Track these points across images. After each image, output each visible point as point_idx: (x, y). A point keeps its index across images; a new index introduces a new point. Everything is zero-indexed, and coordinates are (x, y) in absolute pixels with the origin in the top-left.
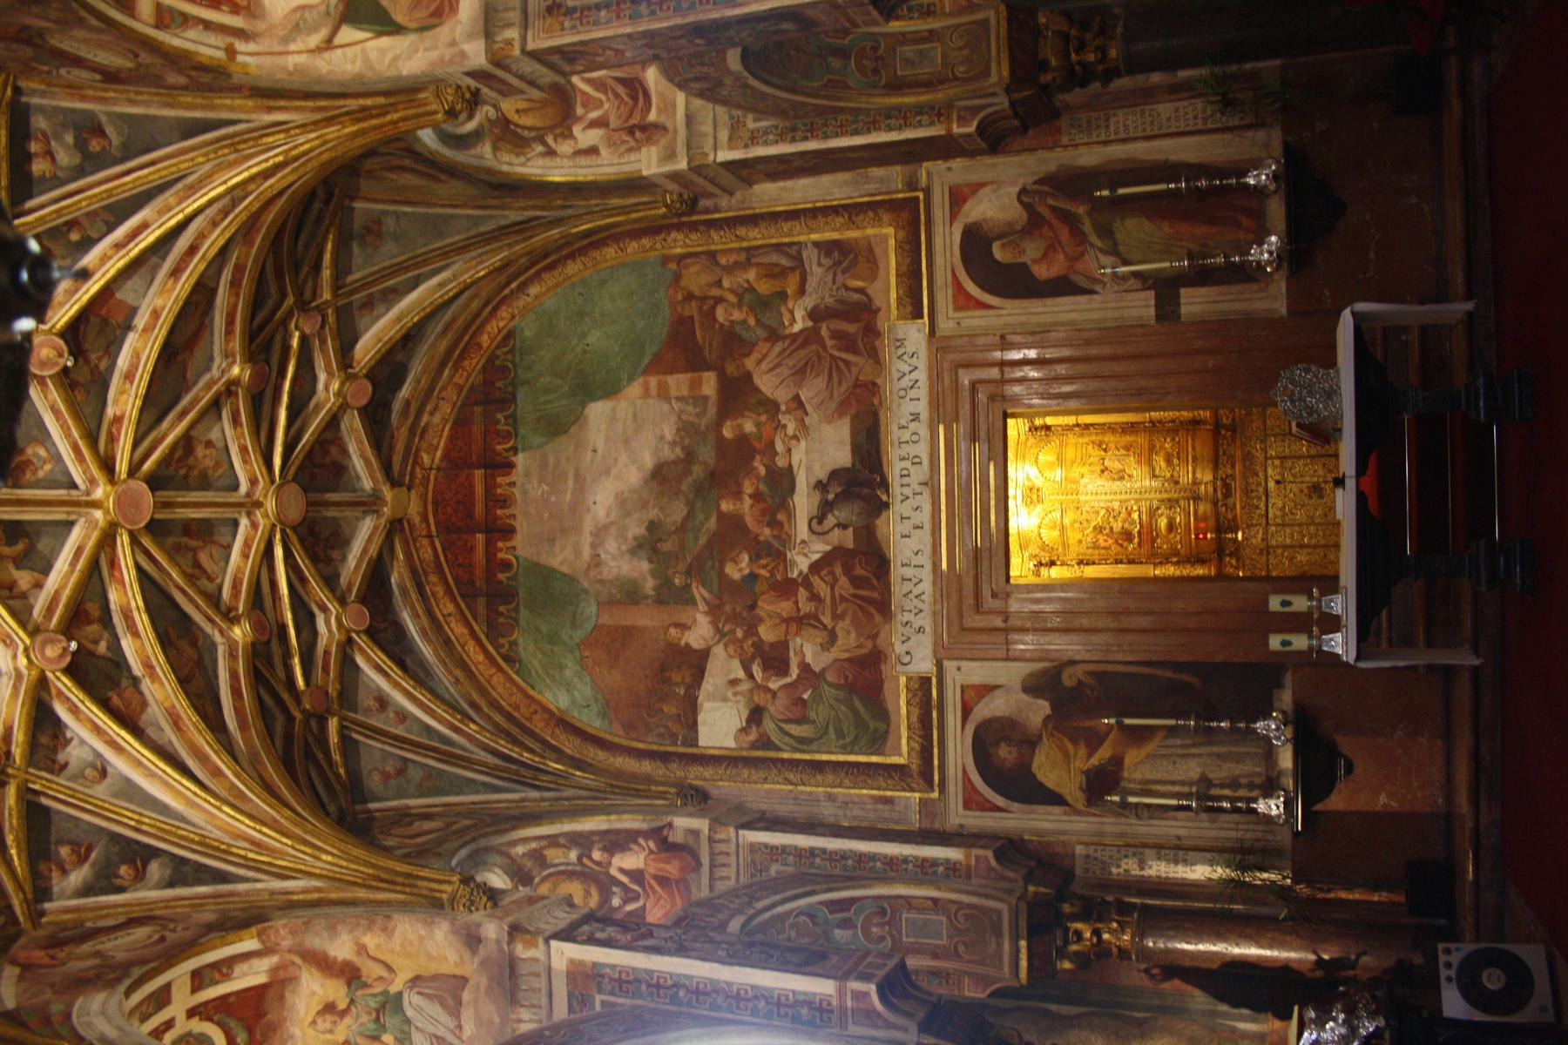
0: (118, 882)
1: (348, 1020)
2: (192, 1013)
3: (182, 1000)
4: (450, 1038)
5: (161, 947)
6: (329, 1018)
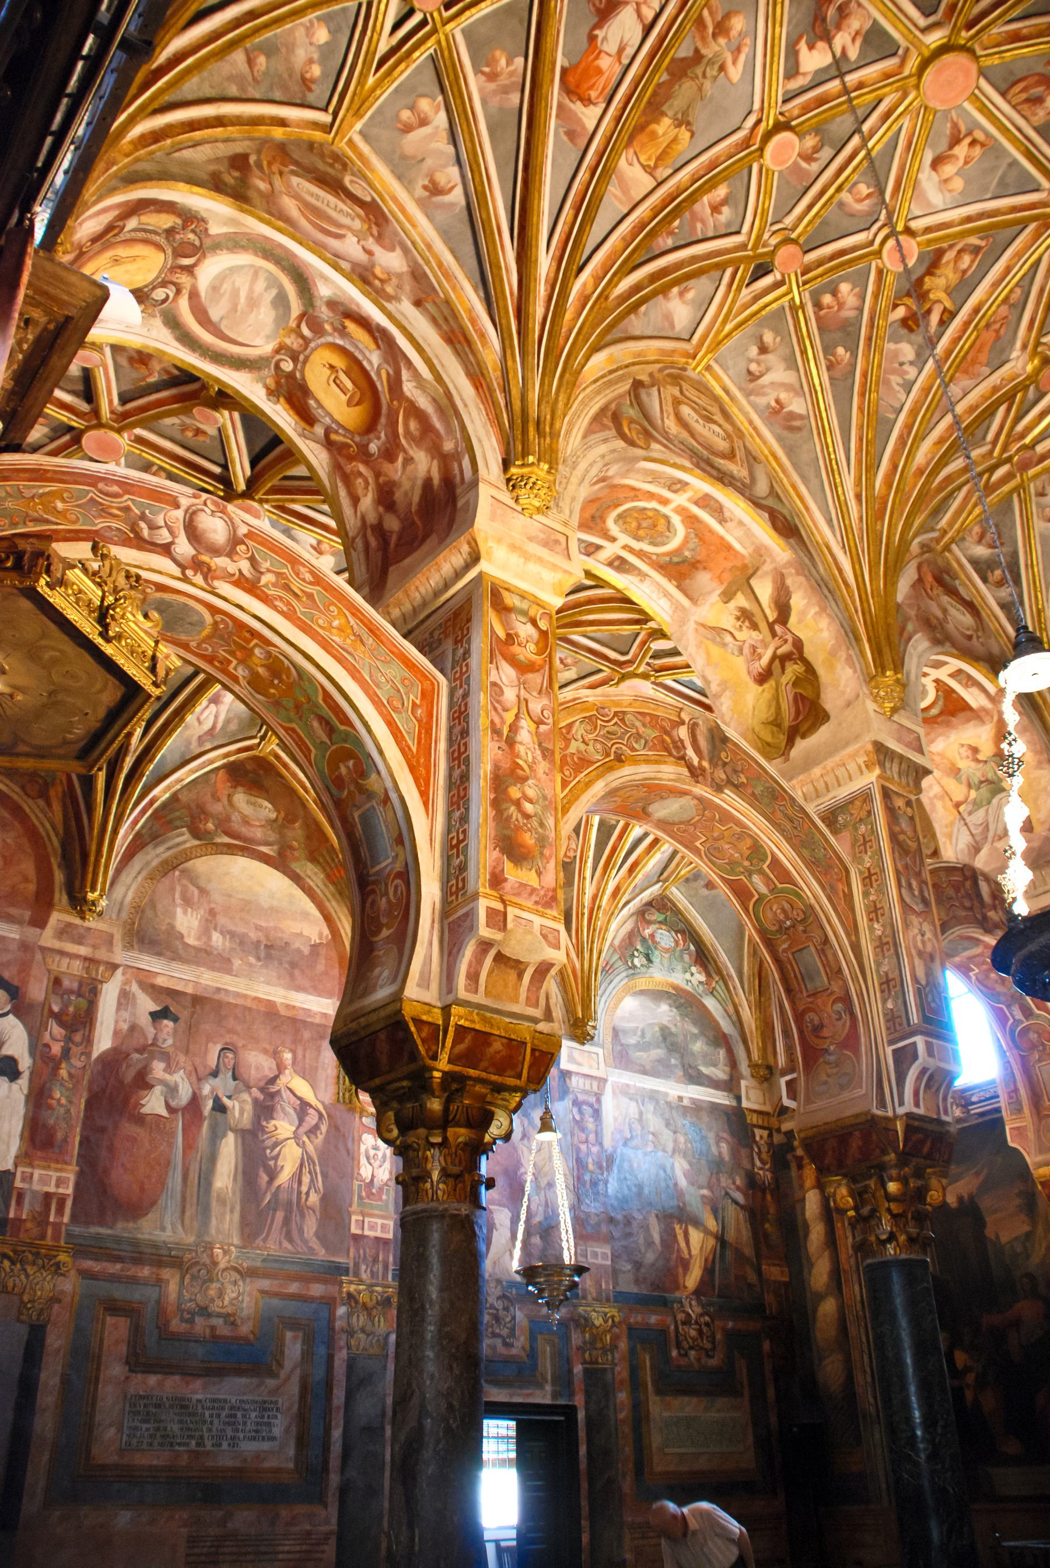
0: (989, 574)
1: (973, 764)
2: (937, 681)
3: (943, 674)
4: (991, 834)
5: (966, 642)
6: (969, 753)
